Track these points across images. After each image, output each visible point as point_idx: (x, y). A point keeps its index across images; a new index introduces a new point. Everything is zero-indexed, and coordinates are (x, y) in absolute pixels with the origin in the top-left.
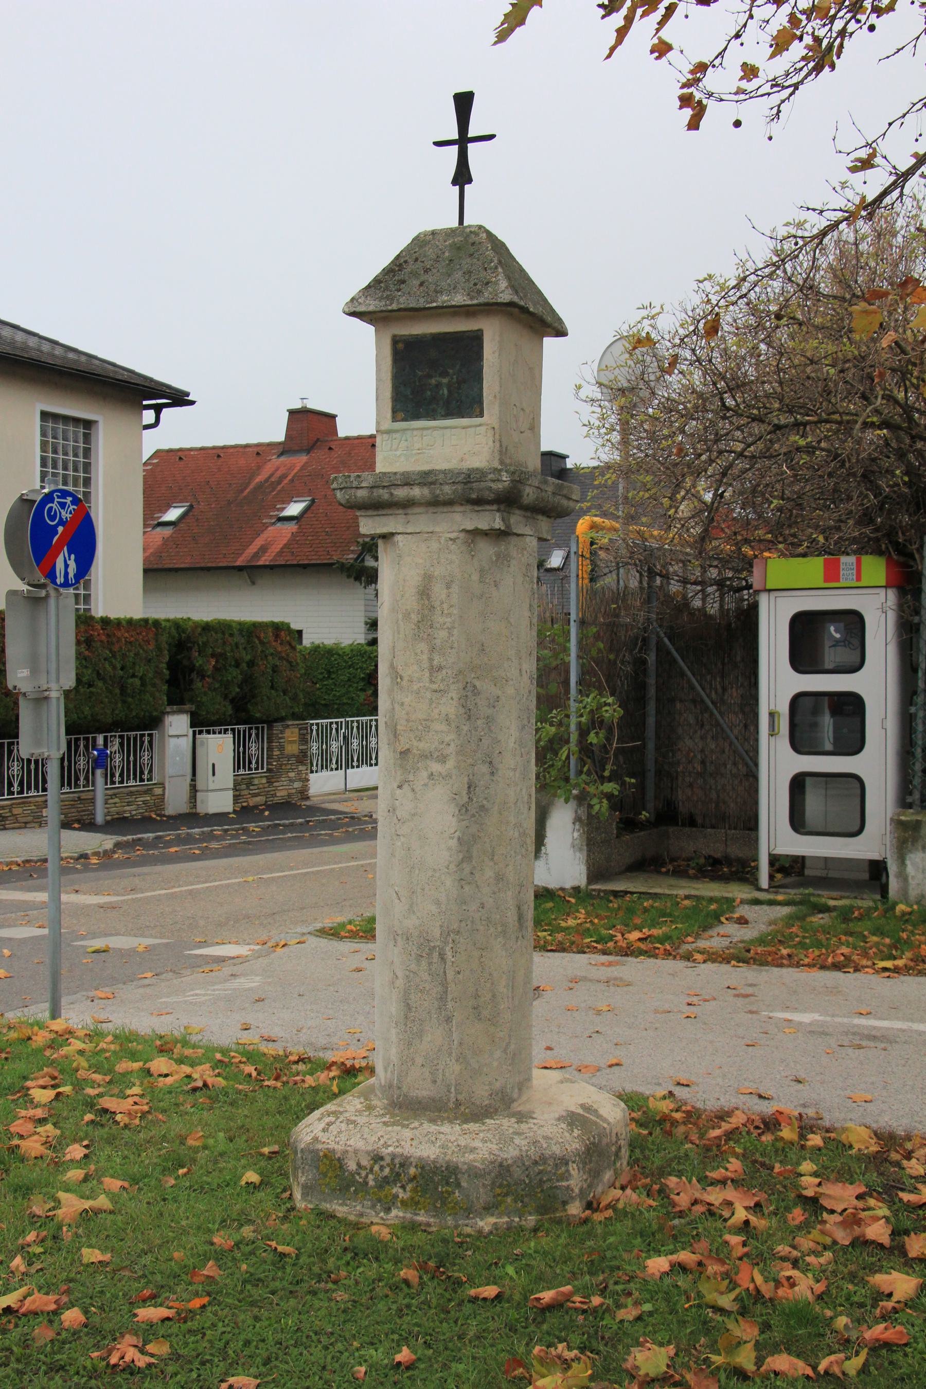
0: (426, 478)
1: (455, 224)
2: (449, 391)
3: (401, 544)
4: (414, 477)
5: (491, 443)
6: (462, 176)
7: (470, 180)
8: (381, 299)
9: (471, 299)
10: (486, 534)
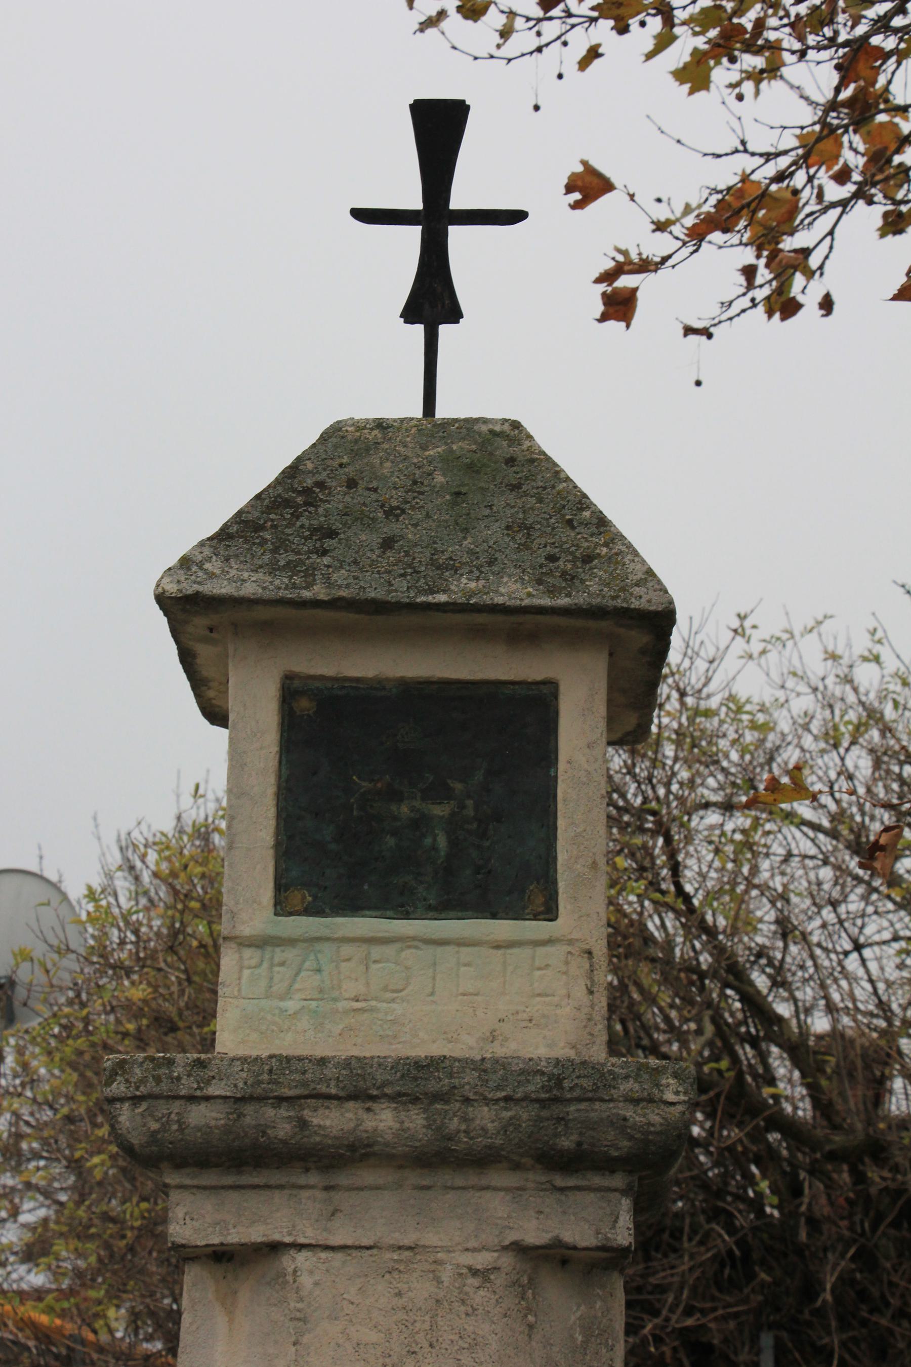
0: (419, 1081)
1: (417, 411)
2: (454, 843)
3: (306, 1281)
4: (381, 1076)
5: (579, 992)
6: (432, 301)
7: (454, 315)
8: (273, 569)
9: (552, 591)
10: (564, 1262)
